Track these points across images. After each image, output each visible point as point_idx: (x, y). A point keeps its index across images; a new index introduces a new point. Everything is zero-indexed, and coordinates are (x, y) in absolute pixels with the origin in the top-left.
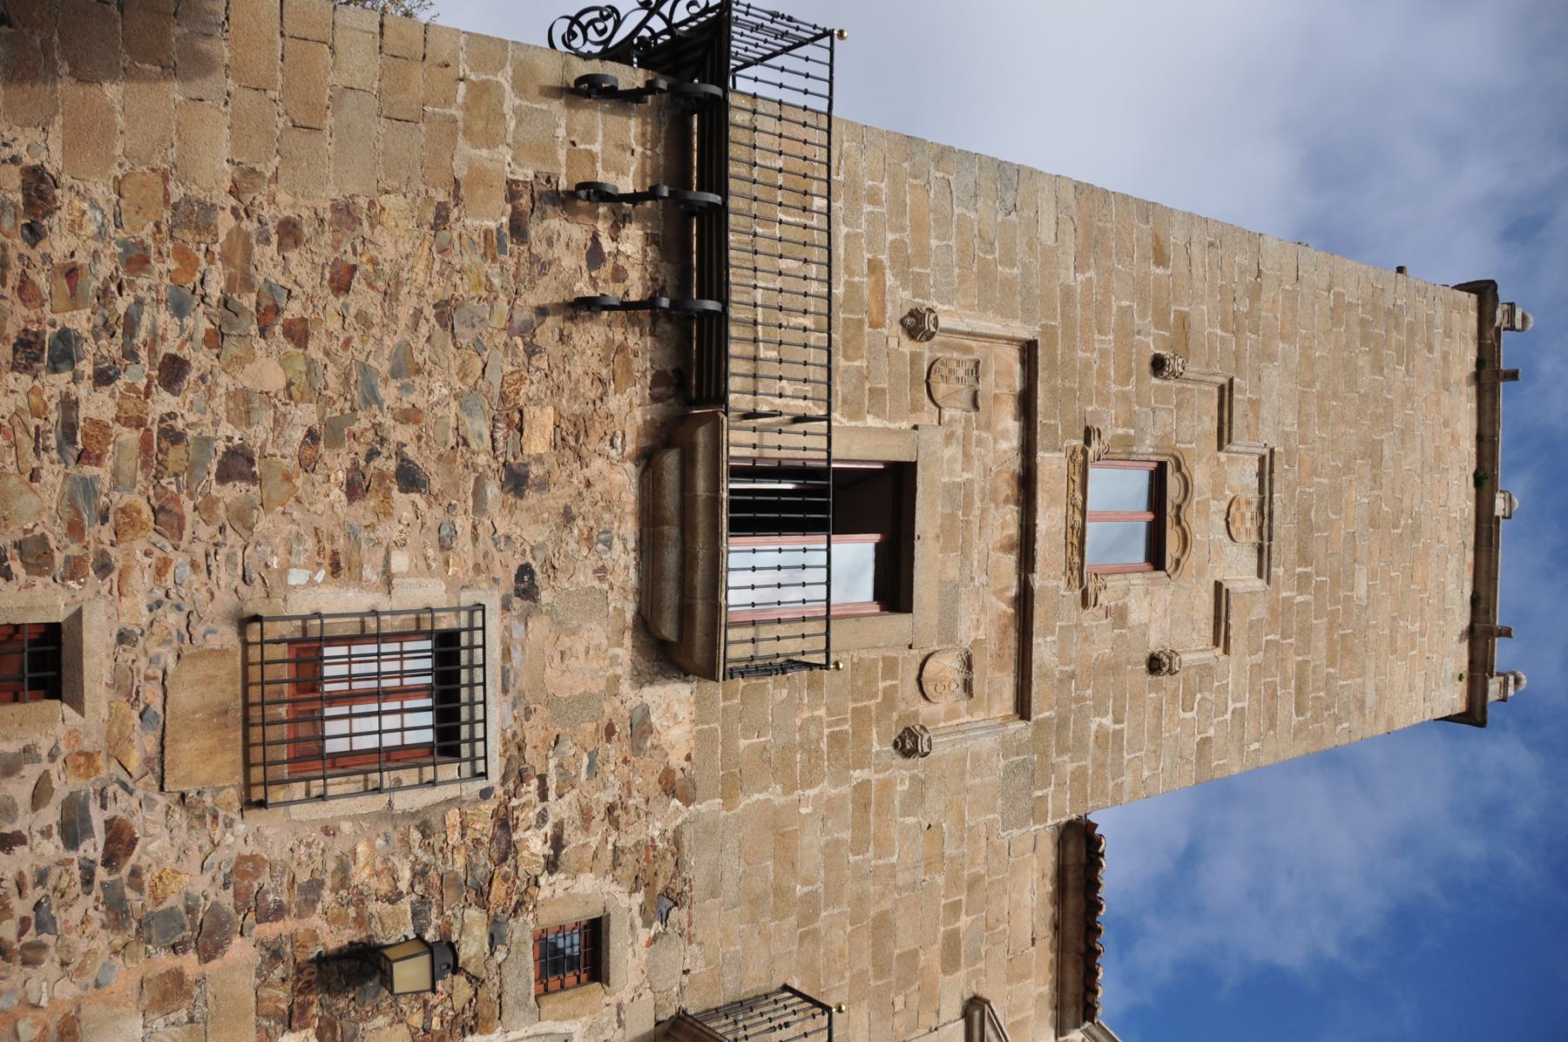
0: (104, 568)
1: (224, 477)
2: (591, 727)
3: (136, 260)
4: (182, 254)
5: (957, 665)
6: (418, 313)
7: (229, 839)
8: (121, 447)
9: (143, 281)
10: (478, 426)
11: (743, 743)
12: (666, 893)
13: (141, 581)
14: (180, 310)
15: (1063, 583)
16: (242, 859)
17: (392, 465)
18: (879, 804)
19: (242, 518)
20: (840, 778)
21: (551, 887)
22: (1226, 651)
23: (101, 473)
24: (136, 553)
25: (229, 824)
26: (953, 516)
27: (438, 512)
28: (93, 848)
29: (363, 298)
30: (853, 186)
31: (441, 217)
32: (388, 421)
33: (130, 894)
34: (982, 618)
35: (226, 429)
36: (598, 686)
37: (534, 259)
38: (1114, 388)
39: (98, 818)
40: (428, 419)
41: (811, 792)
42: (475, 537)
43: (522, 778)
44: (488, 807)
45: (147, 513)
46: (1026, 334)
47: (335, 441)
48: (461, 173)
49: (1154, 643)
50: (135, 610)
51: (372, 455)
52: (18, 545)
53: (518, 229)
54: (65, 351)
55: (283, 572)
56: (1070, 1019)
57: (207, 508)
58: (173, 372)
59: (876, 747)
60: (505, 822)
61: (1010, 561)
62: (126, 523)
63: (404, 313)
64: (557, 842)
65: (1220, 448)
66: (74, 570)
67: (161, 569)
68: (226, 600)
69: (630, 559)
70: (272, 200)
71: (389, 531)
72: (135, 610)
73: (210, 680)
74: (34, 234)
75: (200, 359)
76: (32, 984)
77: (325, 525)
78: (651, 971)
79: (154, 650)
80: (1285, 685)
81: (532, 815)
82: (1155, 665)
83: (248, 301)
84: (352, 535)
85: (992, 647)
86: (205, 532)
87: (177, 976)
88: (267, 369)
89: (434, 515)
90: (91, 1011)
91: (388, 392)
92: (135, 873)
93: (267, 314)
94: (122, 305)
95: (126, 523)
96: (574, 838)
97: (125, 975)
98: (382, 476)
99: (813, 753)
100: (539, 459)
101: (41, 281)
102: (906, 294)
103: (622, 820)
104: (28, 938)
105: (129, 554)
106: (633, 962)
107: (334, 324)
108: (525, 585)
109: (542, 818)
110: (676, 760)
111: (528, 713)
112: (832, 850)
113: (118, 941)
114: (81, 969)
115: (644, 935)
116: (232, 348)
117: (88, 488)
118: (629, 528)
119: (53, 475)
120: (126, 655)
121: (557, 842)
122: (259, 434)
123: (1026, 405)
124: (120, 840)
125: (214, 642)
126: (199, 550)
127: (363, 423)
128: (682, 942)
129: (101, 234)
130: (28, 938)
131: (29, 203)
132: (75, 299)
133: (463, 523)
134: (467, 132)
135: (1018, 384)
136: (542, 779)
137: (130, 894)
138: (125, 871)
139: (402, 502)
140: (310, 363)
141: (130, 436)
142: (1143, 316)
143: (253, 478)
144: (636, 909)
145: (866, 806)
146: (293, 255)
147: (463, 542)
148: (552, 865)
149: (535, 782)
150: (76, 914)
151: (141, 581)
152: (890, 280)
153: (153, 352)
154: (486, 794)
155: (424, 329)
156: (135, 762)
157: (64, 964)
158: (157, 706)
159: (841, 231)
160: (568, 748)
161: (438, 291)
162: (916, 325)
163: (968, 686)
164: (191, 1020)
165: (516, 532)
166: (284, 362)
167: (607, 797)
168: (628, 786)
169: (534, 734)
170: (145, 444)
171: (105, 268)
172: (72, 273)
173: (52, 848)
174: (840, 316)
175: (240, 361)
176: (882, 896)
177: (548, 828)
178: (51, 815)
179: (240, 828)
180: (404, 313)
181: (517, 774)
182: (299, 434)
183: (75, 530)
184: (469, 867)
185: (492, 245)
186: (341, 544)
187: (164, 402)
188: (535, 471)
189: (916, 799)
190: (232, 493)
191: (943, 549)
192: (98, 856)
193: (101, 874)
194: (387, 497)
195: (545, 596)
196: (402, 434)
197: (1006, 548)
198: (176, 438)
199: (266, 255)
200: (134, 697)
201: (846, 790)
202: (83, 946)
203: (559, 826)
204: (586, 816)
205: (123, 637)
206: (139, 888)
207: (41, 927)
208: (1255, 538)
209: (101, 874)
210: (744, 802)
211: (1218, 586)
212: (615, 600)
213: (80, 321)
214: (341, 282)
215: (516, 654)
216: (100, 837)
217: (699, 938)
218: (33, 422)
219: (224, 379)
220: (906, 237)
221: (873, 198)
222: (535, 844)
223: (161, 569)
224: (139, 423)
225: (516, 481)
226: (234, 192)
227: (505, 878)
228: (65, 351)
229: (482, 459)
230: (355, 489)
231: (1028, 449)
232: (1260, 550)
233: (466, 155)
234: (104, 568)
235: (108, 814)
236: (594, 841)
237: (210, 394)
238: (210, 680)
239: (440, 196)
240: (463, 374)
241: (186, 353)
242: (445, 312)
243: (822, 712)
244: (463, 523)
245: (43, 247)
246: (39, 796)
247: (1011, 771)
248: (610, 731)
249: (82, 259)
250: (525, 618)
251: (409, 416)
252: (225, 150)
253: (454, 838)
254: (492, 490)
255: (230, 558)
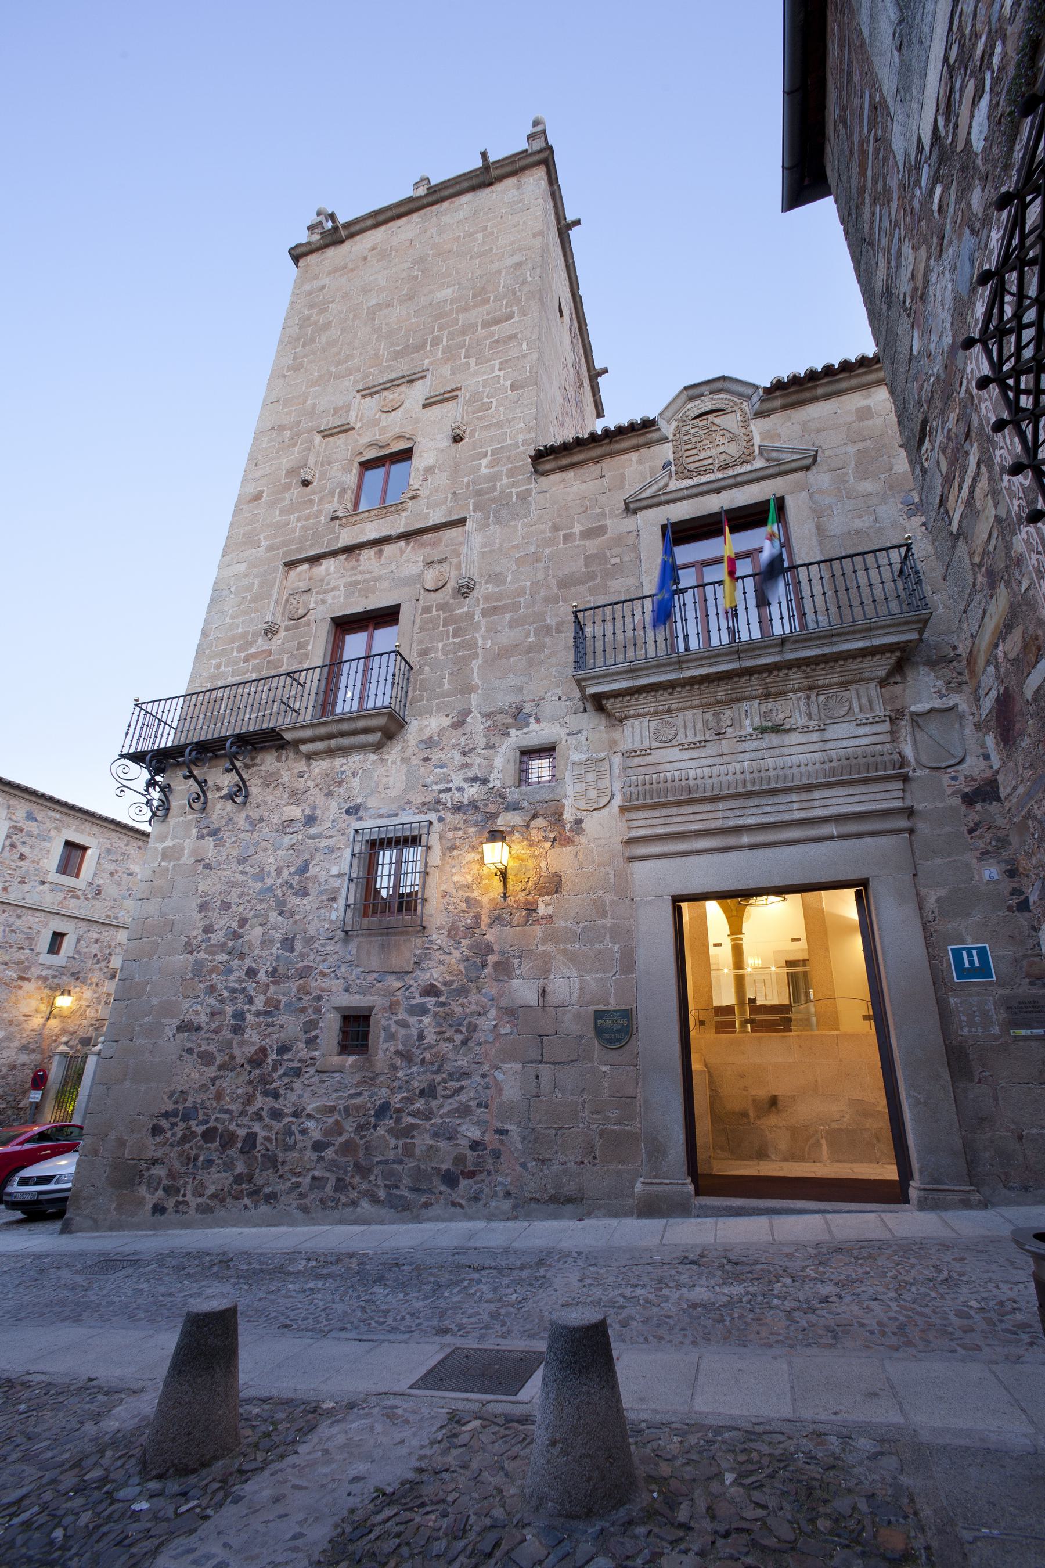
0: (319, 998)
1: (292, 950)
2: (422, 769)
3: (212, 989)
4: (210, 972)
5: (431, 570)
6: (242, 872)
7: (439, 942)
8: (275, 993)
9: (219, 987)
10: (287, 840)
11: (446, 687)
12: (515, 717)
13: (326, 983)
14: (230, 971)
15: (404, 514)
16: (449, 936)
17: (297, 877)
18: (496, 600)
19: (309, 941)
20: (477, 627)
21: (495, 782)
22: (459, 389)
23: (283, 999)
24: (316, 984)
25: (431, 942)
26: (359, 591)
27: (318, 855)
28: (430, 1001)
29: (233, 898)
30: (214, 677)
31: (208, 867)
32: (280, 881)
33: (454, 986)
34: (407, 560)
35: (274, 950)
36: (404, 768)
37: (227, 824)
38: (315, 508)
39: (418, 1000)
40: (281, 863)
41: (480, 641)
42: (331, 837)
43: (438, 802)
44: (449, 817)
45: (301, 981)
46: (281, 567)
47: (283, 903)
48: (193, 860)
49: (447, 443)
50: (337, 985)
51: (291, 887)
52: (306, 1033)
53: (214, 833)
54: (239, 1016)
55: (331, 922)
56: (655, 436)
57: (303, 956)
58: (251, 973)
59: (465, 609)
60: (458, 808)
61: (388, 549)
62: (304, 990)
63: (240, 878)
64: (475, 779)
65: (353, 429)
66: (318, 1010)
67: (323, 975)
68: (338, 947)
69: (351, 759)
70: (195, 937)
71: (323, 876)
72: (337, 985)
73: (369, 953)
74: (198, 1029)
75: (248, 962)
76: (485, 1028)
77: (317, 905)
78: (554, 719)
79: (353, 977)
80: (493, 334)
81: (457, 794)
82: (457, 439)
83: (230, 944)
84: (322, 893)
85: (427, 550)
86: (311, 958)
87: (497, 964)
88: (254, 933)
89: (319, 856)
90: (504, 1003)
91: (269, 882)
92: (445, 984)
93: (236, 936)
94: (226, 994)
95: (304, 990)
96: (476, 771)
97: (491, 988)
98: (300, 882)
99: (462, 646)
100: (303, 811)
101: (214, 1025)
102: (260, 640)
103: (471, 746)
104: (464, 1030)
105: (315, 988)
106: (547, 730)
107: (242, 907)
108: (353, 811)
109: (460, 789)
110: (447, 722)
111: (409, 802)
112: (514, 624)
113: (475, 991)
114: (483, 1007)
115: (533, 725)
116: (245, 950)
117: (289, 1004)
118: (338, 762)
119: (282, 1019)
120: (354, 989)
121: (475, 779)
122: (277, 936)
123: (314, 560)
124: (431, 990)
125: (354, 951)
126: (319, 959)
127: (279, 893)
128: (543, 703)
129: (201, 1004)
130: (464, 1030)
131: (188, 1031)
132: (222, 1012)
133: (324, 843)
134: (179, 859)
135: (306, 566)
136: (441, 791)
137: (454, 986)
138: (443, 988)
139: (312, 871)
140: (254, 916)
141: (272, 989)
142: (284, 499)
143: (293, 938)
144: (519, 733)
145: (495, 608)
146: (216, 927)
147: (331, 842)
148: (485, 781)
149: (442, 795)
150: (458, 1010)
151: (326, 983)
152: (252, 650)
153: (244, 981)
154: (441, 820)
155: (247, 869)
156: (398, 984)
157: (479, 1014)
158: (376, 975)
159: (231, 680)
160: (428, 781)
161: (234, 866)
162: (270, 632)
163: (441, 561)
164: (520, 957)
165: (332, 818)
166: (253, 927)
167: (457, 755)
168: (454, 746)
169: (418, 798)
170: (275, 983)
171: (212, 1001)
172: (213, 1014)
173: (427, 1020)
174: (265, 673)
175: (251, 945)
176: (548, 586)
177: (465, 786)
178: (413, 1020)
179: (434, 937)
180: (240, 878)
181: (436, 804)
182: (280, 918)
183: (303, 1010)
184: (476, 824)
185: (219, 843)
186: (325, 897)
187: (262, 976)
188: (307, 813)
189: (496, 578)
190: (298, 946)
191: (374, 592)
192: (433, 1000)
193: (442, 999)
194: (308, 878)
195: (359, 800)
196: (285, 873)
197: (381, 552)
198: (275, 970)
199: (214, 938)
200: (372, 985)
201: (483, 622)
202: (473, 1007)
203: (465, 780)
204: (465, 766)
205: (347, 990)
206: (452, 982)
207: (460, 1024)
208: (403, 388)
209: (442, 999)
210: (477, 681)
211: (425, 406)
212: (368, 765)
213: (229, 1010)
214: (226, 906)
215: (381, 811)
216: (427, 999)
217: (542, 694)
218: (263, 1027)
219: (256, 952)
220: (236, 645)
221: (218, 666)
222: (473, 791)
223: (323, 975)
224: (268, 985)
225: (310, 820)
226: (191, 952)
227: (486, 805)
228: (239, 1016)
229: (300, 837)
230: (304, 893)
231: (334, 554)
232: (411, 381)
233: (187, 859)
234: (319, 998)
235: (417, 995)
236: (478, 760)
237: (261, 957)
238: (369, 953)
239: (200, 868)
240: (265, 850)
241: (245, 968)
242: (242, 861)
243: (440, 645)
244: (324, 843)
245: (203, 1025)
246: (405, 1025)
247: (498, 520)
248: (427, 759)
249: (208, 1011)
250: (367, 809)
251: (279, 871)
252: (177, 957)
253: (460, 833)
254: (313, 831)
255: (323, 946)
